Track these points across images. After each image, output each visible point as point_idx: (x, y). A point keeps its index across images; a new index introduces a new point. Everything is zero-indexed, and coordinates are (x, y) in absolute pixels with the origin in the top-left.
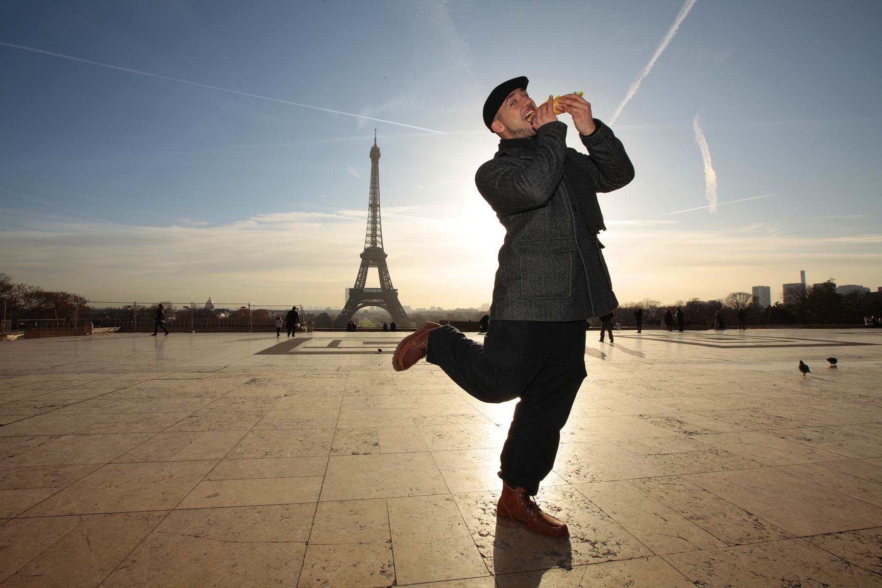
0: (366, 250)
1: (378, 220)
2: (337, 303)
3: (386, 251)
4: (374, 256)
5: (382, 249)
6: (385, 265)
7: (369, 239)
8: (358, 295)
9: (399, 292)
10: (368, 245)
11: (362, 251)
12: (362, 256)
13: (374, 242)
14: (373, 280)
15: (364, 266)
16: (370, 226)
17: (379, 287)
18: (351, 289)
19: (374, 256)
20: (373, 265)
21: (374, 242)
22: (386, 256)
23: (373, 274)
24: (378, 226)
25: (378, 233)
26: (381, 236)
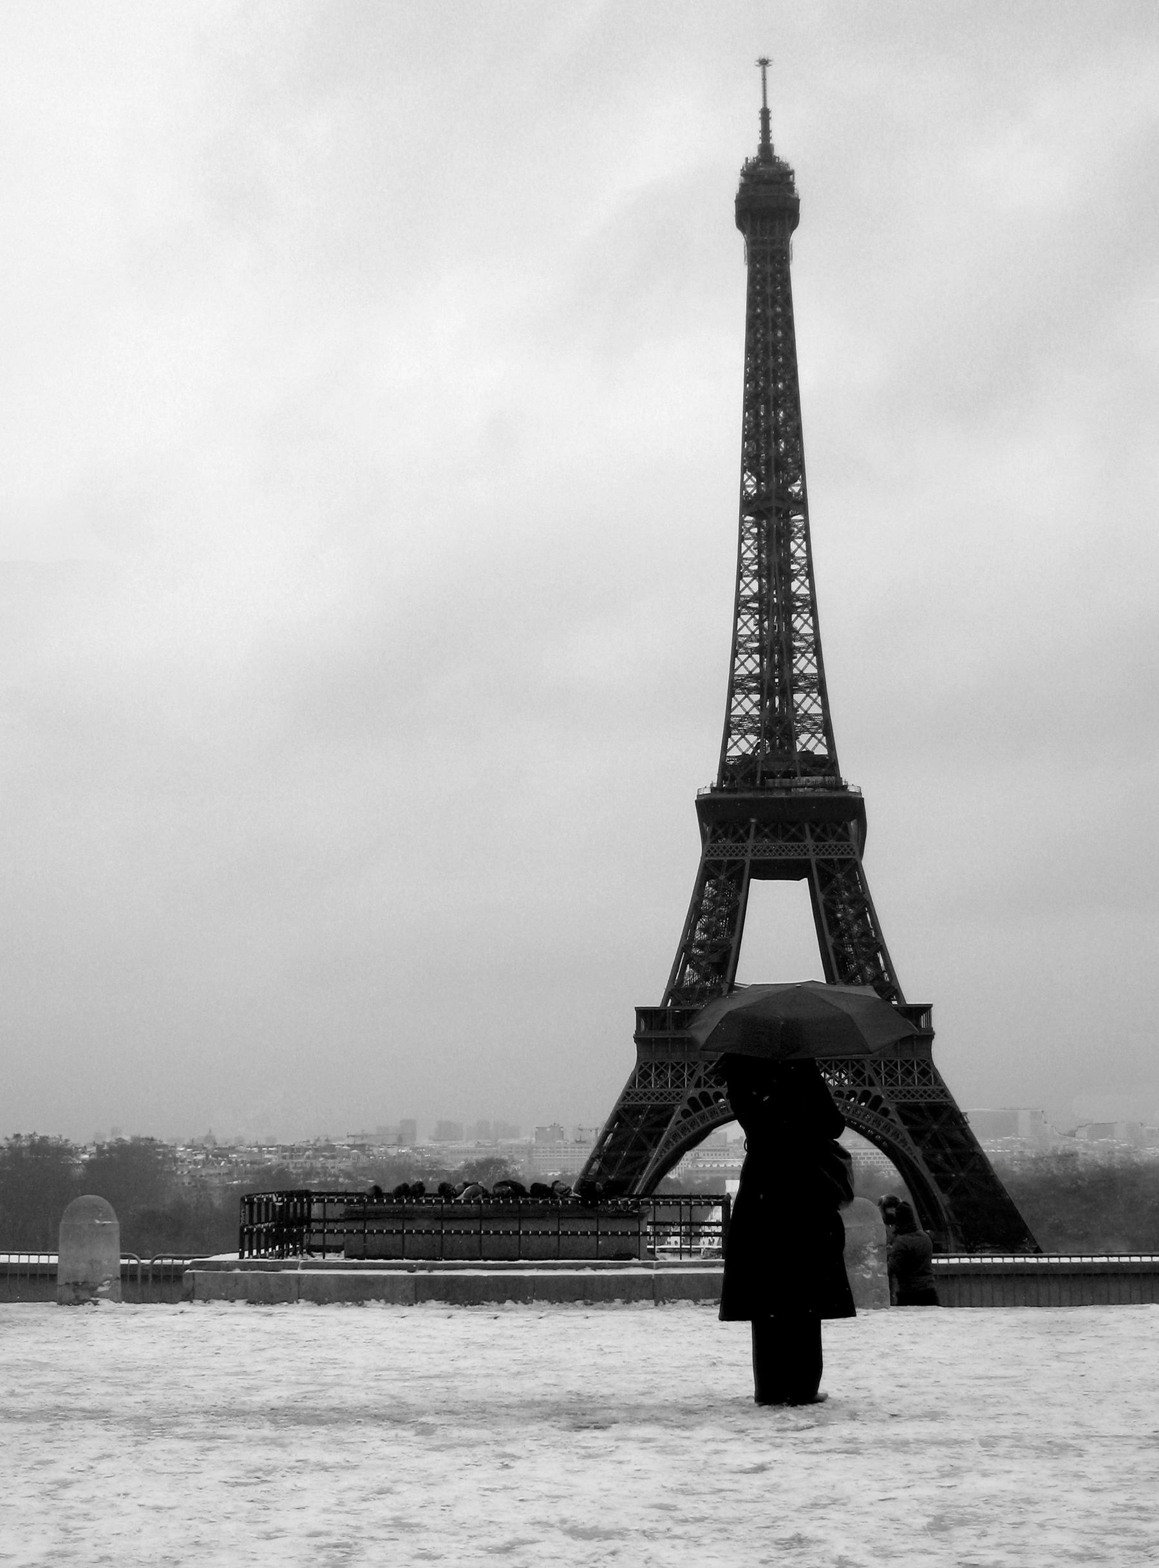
0: (732, 772)
1: (798, 587)
3: (852, 774)
4: (781, 809)
5: (829, 765)
7: (748, 705)
9: (938, 1022)
10: (743, 745)
11: (707, 777)
13: (778, 726)
16: (749, 625)
19: (781, 809)
21: (778, 726)
24: (801, 624)
25: (804, 665)
26: (819, 685)
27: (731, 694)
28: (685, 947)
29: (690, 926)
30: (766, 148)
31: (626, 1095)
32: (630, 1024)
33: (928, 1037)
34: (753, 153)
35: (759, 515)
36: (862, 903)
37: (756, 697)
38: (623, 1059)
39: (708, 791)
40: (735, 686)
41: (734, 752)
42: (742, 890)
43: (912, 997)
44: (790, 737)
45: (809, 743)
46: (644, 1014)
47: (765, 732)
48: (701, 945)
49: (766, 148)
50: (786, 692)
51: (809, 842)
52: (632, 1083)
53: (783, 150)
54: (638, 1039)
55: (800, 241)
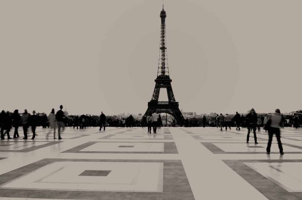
0: (159, 77)
2: (139, 110)
4: (163, 81)
6: (171, 87)
7: (160, 70)
8: (154, 105)
9: (179, 104)
10: (160, 74)
11: (156, 78)
12: (155, 81)
13: (163, 72)
14: (163, 97)
15: (158, 87)
17: (168, 101)
18: (148, 103)
19: (163, 81)
20: (163, 87)
21: (163, 72)
22: (171, 81)
23: (163, 91)
24: (166, 61)
25: (166, 66)
27: (158, 68)
28: (153, 95)
29: (154, 93)
30: (163, 9)
31: (147, 111)
32: (147, 104)
33: (178, 105)
34: (162, 10)
35: (162, 49)
36: (172, 92)
37: (161, 69)
38: (147, 107)
39: (156, 79)
40: (159, 68)
41: (158, 75)
42: (159, 89)
43: (177, 102)
44: (165, 73)
45: (166, 74)
46: (148, 103)
47: (162, 73)
48: (155, 95)
49: (163, 9)
50: (164, 68)
51: (166, 85)
52: (147, 110)
53: (165, 10)
54: (148, 105)
55: (166, 19)
